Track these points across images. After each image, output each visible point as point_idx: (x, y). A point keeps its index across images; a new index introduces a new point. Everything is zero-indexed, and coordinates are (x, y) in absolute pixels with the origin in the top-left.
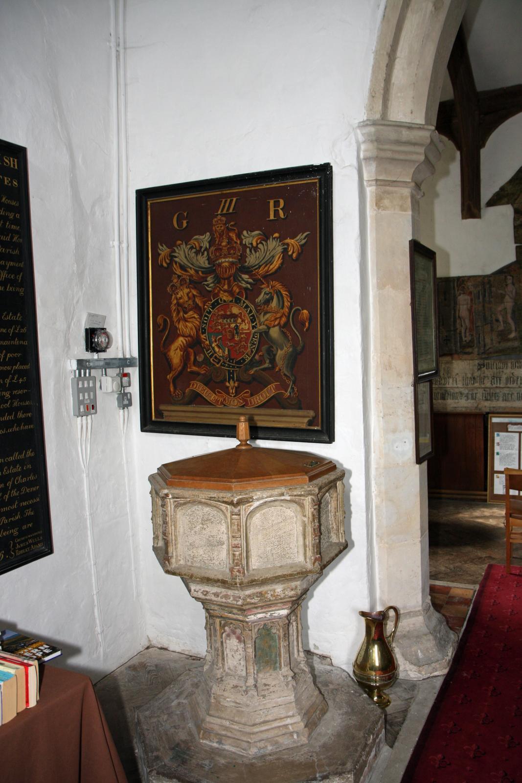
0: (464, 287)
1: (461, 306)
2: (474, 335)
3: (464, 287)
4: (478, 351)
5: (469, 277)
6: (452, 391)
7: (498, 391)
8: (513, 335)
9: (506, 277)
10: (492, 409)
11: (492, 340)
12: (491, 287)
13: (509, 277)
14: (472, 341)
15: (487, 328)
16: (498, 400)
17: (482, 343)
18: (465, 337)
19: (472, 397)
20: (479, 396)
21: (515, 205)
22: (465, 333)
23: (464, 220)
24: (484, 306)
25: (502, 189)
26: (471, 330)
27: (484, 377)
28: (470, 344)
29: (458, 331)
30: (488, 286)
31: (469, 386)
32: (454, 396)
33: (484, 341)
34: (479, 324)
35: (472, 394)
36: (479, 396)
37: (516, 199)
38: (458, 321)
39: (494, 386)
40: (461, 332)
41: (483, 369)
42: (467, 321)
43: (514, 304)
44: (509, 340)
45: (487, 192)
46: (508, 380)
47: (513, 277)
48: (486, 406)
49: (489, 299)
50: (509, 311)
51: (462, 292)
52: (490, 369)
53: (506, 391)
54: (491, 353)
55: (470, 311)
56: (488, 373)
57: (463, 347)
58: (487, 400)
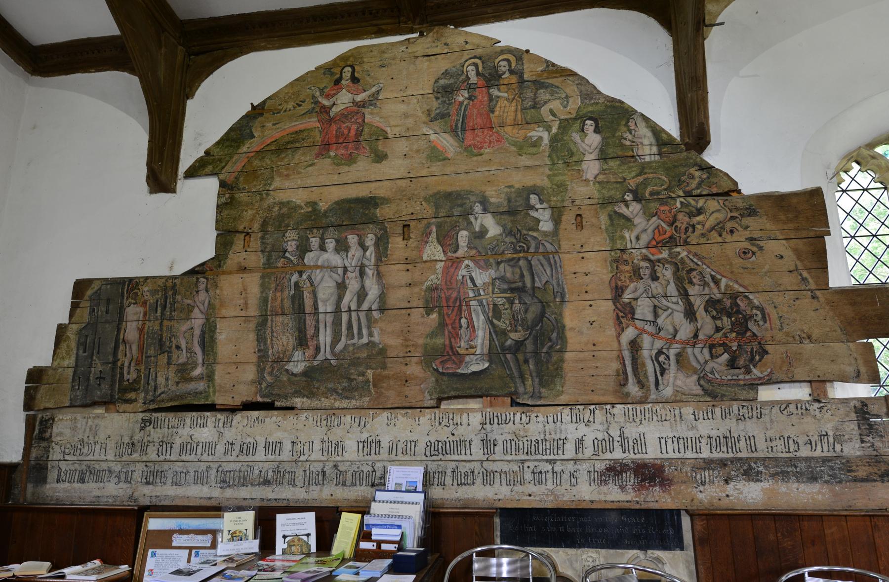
0: (137, 293)
1: (129, 323)
2: (142, 370)
3: (137, 293)
4: (145, 398)
5: (146, 278)
6: (97, 467)
7: (166, 466)
8: (198, 371)
9: (198, 279)
10: (154, 500)
11: (167, 379)
12: (175, 293)
13: (202, 280)
14: (137, 381)
15: (163, 359)
16: (165, 484)
17: (152, 383)
18: (129, 373)
19: (126, 478)
20: (137, 476)
21: (222, 176)
22: (129, 367)
23: (154, 196)
24: (161, 325)
25: (207, 153)
26: (138, 363)
27: (149, 442)
28: (133, 387)
29: (119, 364)
30: (170, 293)
31: (124, 459)
32: (98, 476)
33: (156, 380)
34: (151, 352)
35: (127, 473)
36: (137, 476)
37: (223, 168)
38: (121, 347)
39: (162, 458)
40: (123, 365)
41: (148, 428)
42: (135, 348)
43: (204, 320)
44: (191, 379)
45: (188, 156)
46: (183, 447)
47: (207, 279)
48: (146, 494)
49: (171, 312)
50: (197, 332)
51: (133, 301)
52: (158, 430)
53: (178, 467)
54: (163, 401)
55: (141, 330)
56: (156, 434)
57: (124, 390)
58: (148, 483)
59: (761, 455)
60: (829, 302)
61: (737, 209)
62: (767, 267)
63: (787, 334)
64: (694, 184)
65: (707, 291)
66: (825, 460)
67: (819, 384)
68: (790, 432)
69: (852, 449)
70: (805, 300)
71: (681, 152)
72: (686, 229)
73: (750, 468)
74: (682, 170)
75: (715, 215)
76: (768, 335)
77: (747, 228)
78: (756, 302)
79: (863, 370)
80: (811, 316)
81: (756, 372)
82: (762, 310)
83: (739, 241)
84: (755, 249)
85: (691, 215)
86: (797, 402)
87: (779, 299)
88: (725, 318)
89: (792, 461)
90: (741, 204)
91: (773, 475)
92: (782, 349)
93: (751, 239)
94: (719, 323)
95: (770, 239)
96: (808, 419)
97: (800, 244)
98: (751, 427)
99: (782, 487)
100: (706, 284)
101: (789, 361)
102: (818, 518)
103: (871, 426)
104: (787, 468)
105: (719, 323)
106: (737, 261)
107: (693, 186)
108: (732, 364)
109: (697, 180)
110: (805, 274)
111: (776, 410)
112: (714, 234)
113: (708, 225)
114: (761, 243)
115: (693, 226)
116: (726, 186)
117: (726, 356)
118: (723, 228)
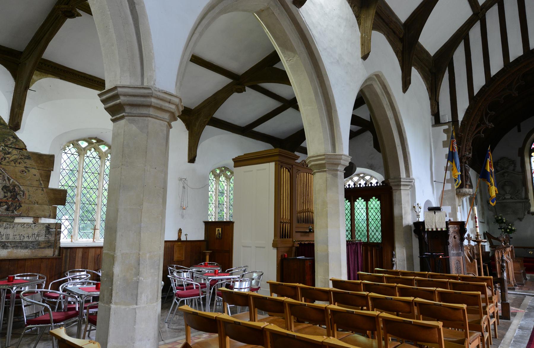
59: (10, 240)
60: (47, 192)
61: (24, 155)
62: (29, 178)
63: (30, 201)
64: (9, 143)
65: (4, 182)
66: (32, 242)
67: (36, 218)
68: (23, 233)
69: (42, 239)
70: (39, 191)
71: (8, 129)
72: (2, 159)
73: (5, 245)
74: (6, 136)
75: (15, 156)
76: (23, 201)
77: (25, 163)
78: (22, 189)
79: (52, 214)
80: (40, 196)
81: (16, 213)
82: (23, 192)
83: (21, 167)
84: (26, 171)
85: (5, 154)
86: (27, 224)
87: (30, 189)
88: (9, 193)
89: (20, 242)
90: (25, 154)
91: (13, 247)
92: (27, 205)
93: (26, 167)
94: (6, 194)
95: (33, 168)
96: (30, 229)
97: (43, 172)
98: (10, 232)
99: (15, 251)
100: (4, 180)
101: (28, 210)
102: (25, 260)
103: (49, 232)
104: (17, 245)
105: (6, 194)
106: (19, 174)
107: (9, 143)
108: (7, 209)
109: (11, 141)
110: (42, 182)
111: (20, 226)
112: (13, 162)
113: (11, 159)
114: (29, 169)
115: (5, 158)
116: (22, 146)
117: (6, 206)
118: (16, 161)
